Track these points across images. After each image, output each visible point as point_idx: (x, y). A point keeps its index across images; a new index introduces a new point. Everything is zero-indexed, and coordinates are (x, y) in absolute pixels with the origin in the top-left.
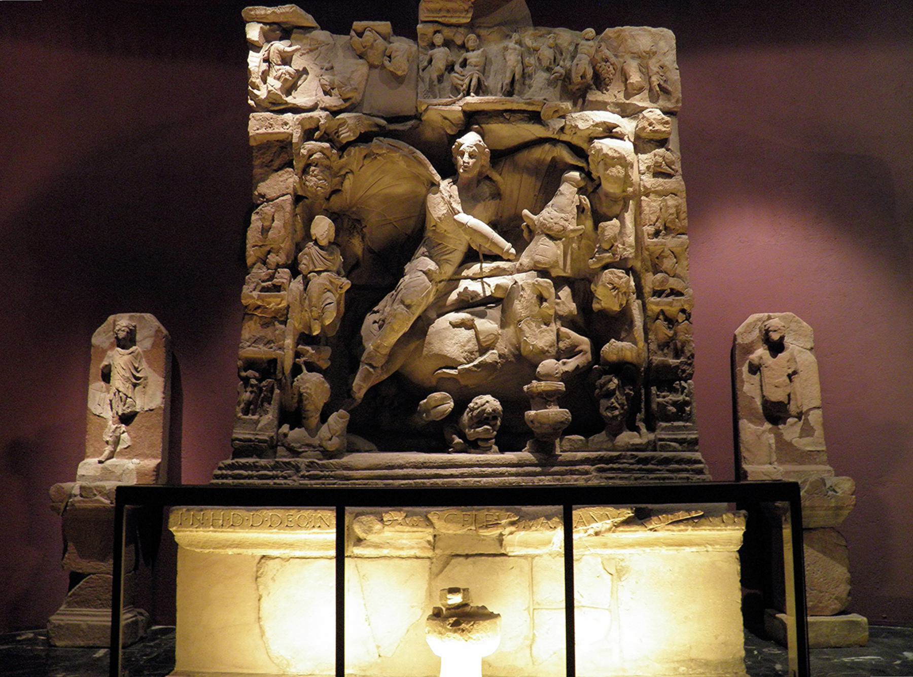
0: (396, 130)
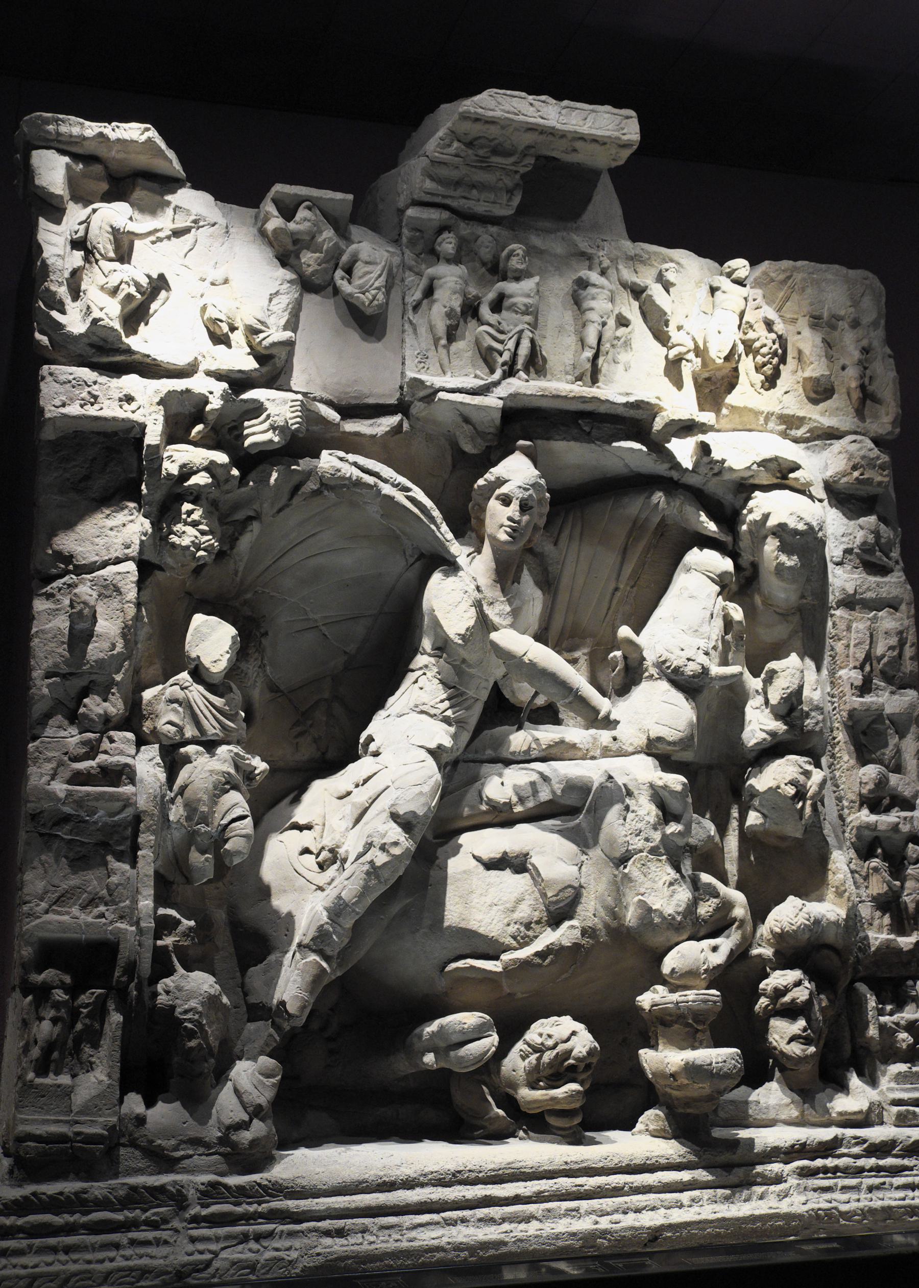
0: (357, 434)
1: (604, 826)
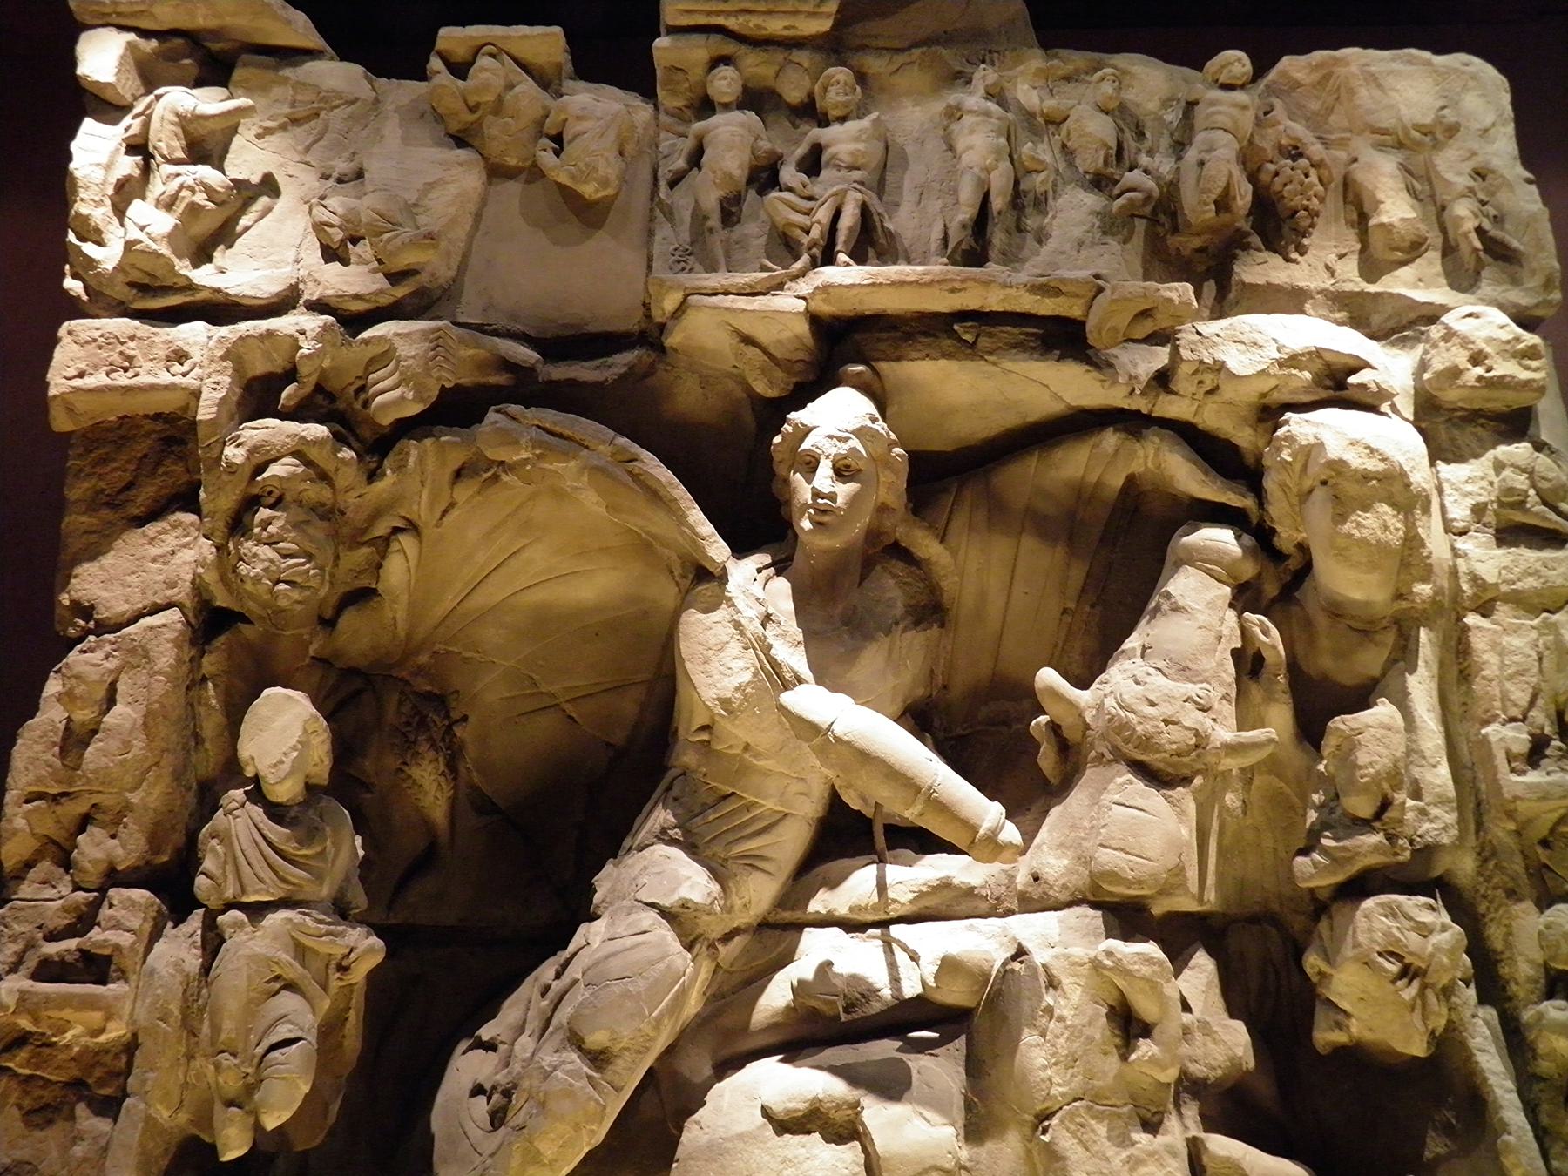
0: (572, 383)
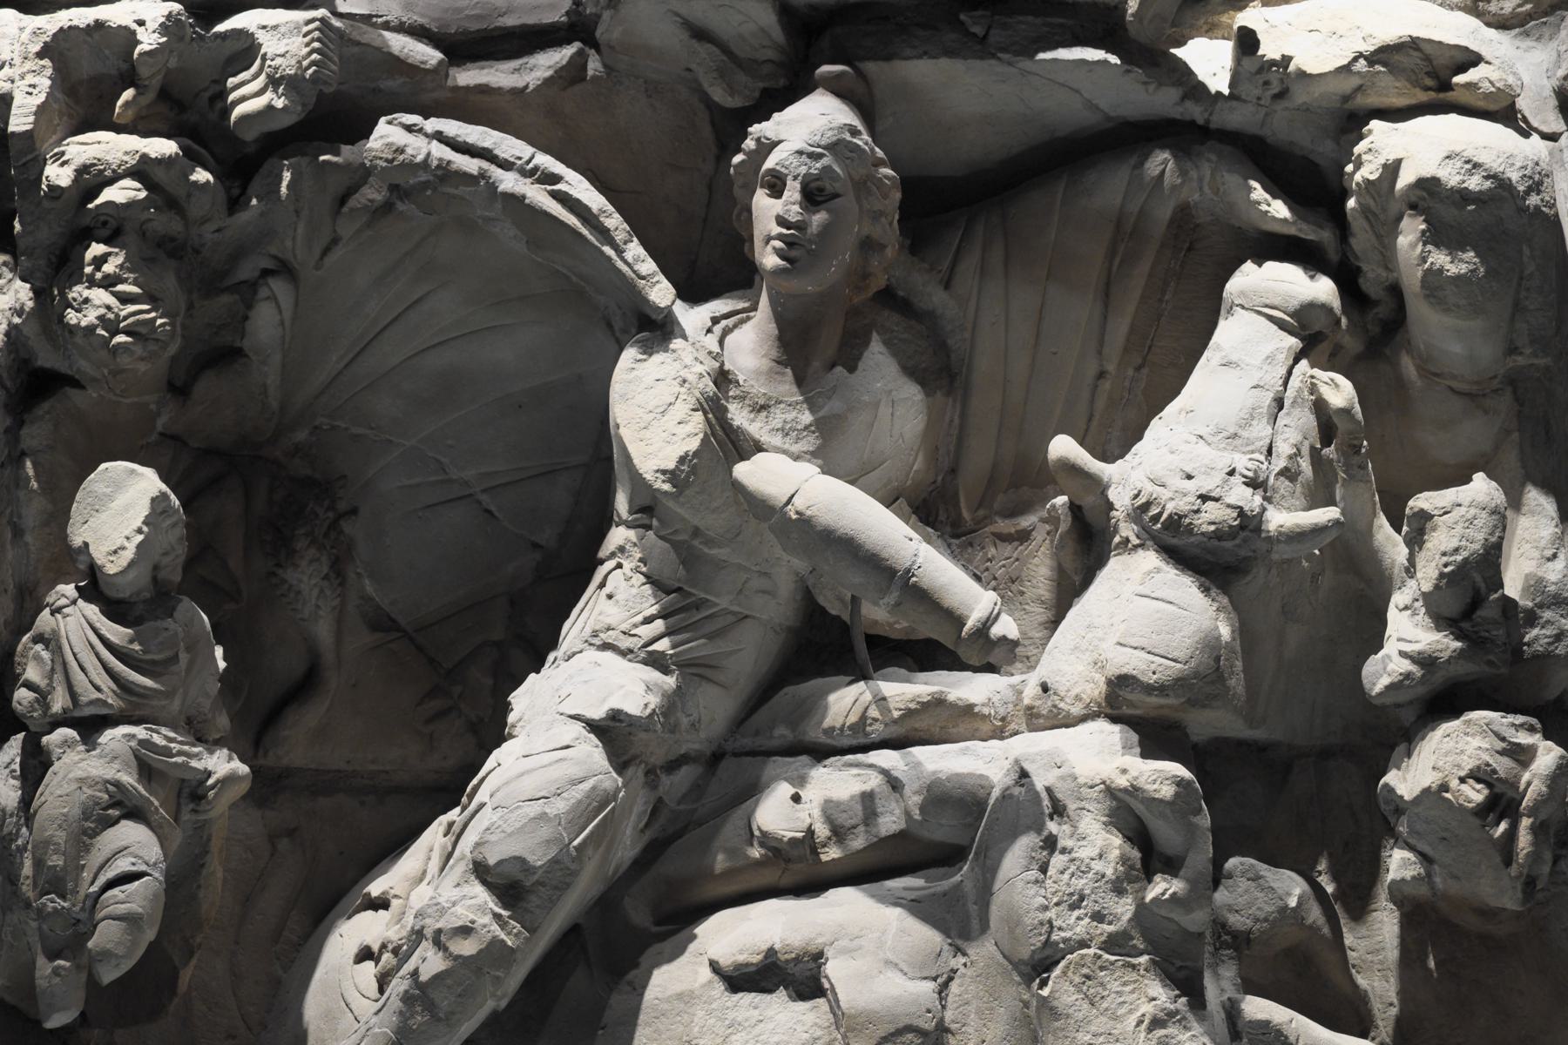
0: (484, 89)
1: (996, 886)
